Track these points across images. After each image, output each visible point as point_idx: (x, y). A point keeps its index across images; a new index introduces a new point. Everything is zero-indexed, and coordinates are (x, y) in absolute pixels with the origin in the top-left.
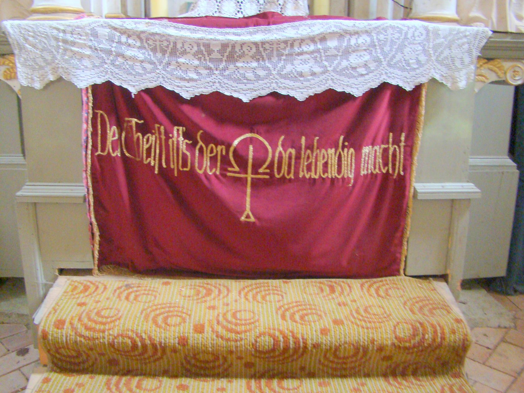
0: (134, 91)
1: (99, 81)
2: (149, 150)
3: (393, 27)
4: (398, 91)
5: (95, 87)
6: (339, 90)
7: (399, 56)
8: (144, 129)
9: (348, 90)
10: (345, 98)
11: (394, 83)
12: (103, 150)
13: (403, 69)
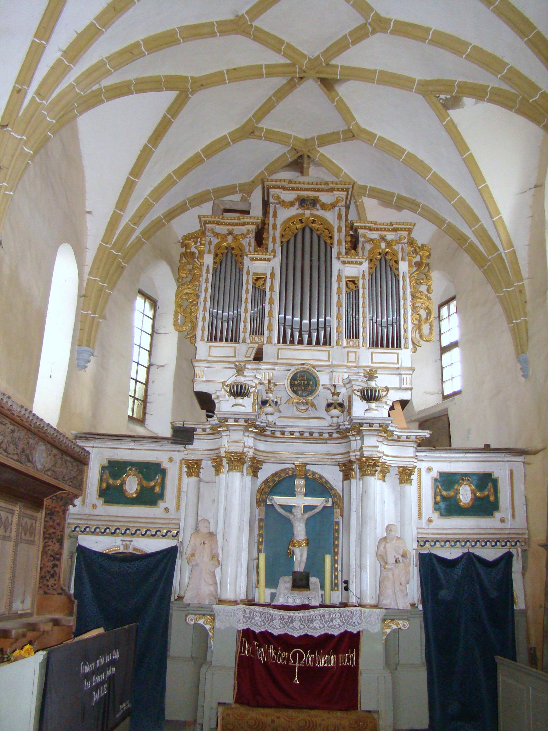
0: (257, 632)
1: (245, 628)
2: (260, 654)
3: (348, 611)
4: (351, 633)
5: (243, 630)
6: (329, 633)
7: (351, 621)
8: (260, 646)
9: (333, 633)
10: (332, 636)
11: (349, 630)
12: (244, 653)
13: (352, 626)
